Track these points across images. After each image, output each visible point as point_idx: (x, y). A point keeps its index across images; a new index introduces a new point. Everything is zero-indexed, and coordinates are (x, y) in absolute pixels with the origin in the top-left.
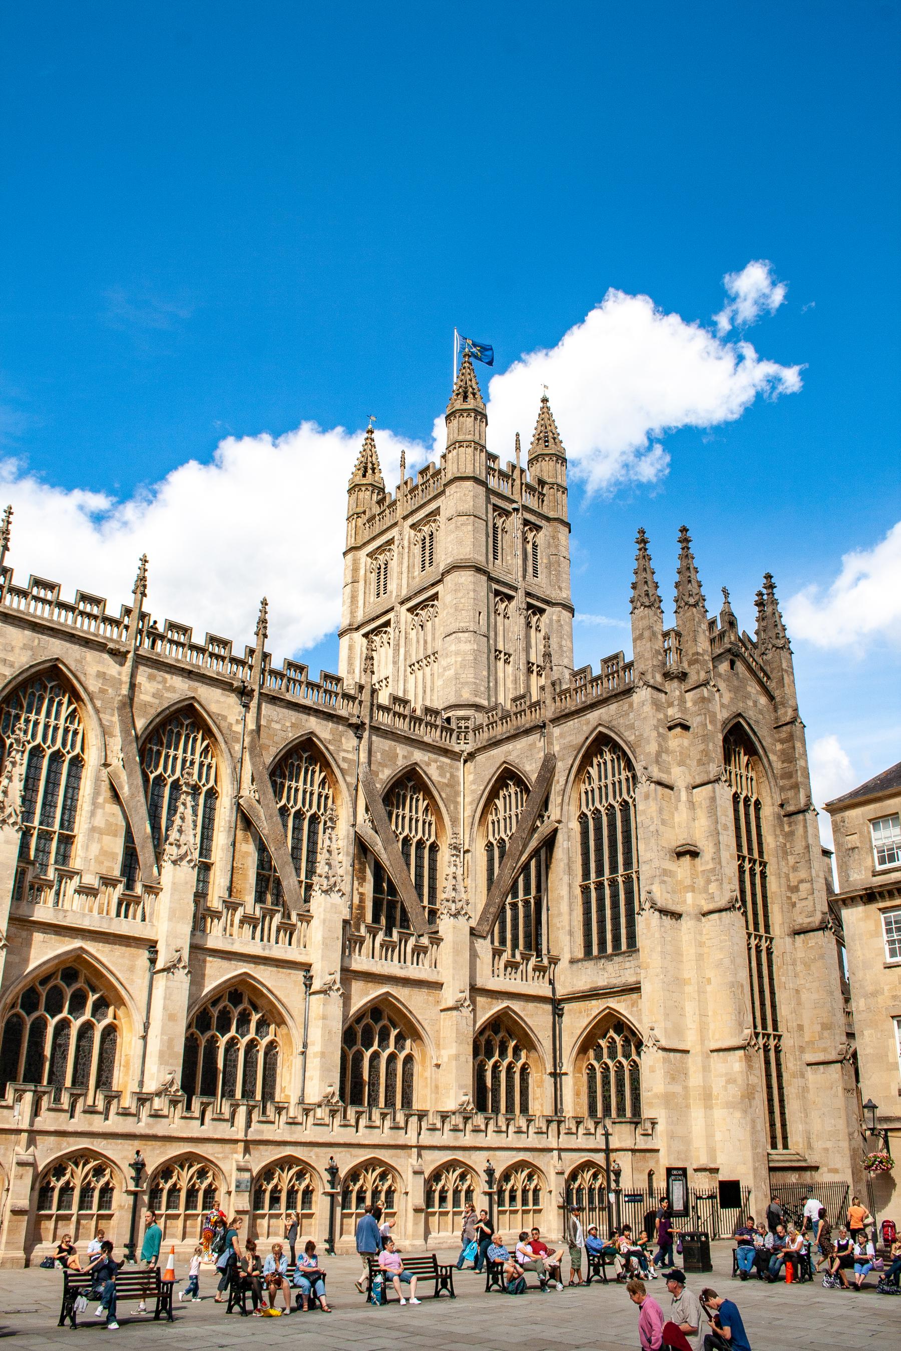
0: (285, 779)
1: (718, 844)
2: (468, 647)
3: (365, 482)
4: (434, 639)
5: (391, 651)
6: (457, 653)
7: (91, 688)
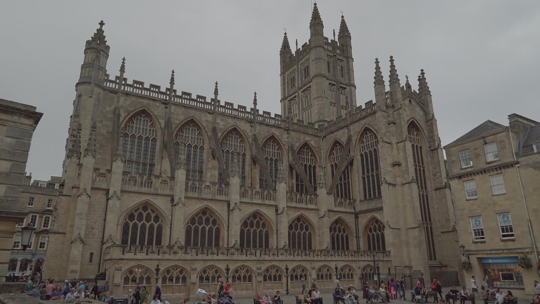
1: (407, 161)
2: (321, 102)
4: (310, 100)
5: (297, 106)
6: (318, 105)
7: (204, 125)
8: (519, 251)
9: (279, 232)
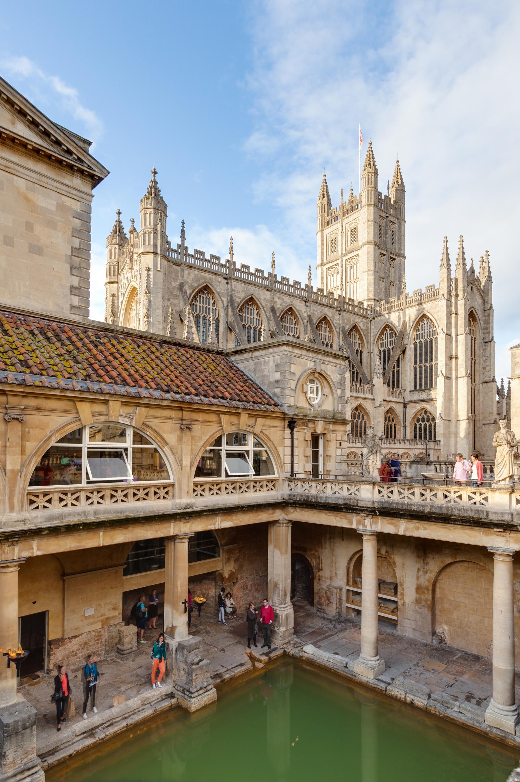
7: (263, 304)
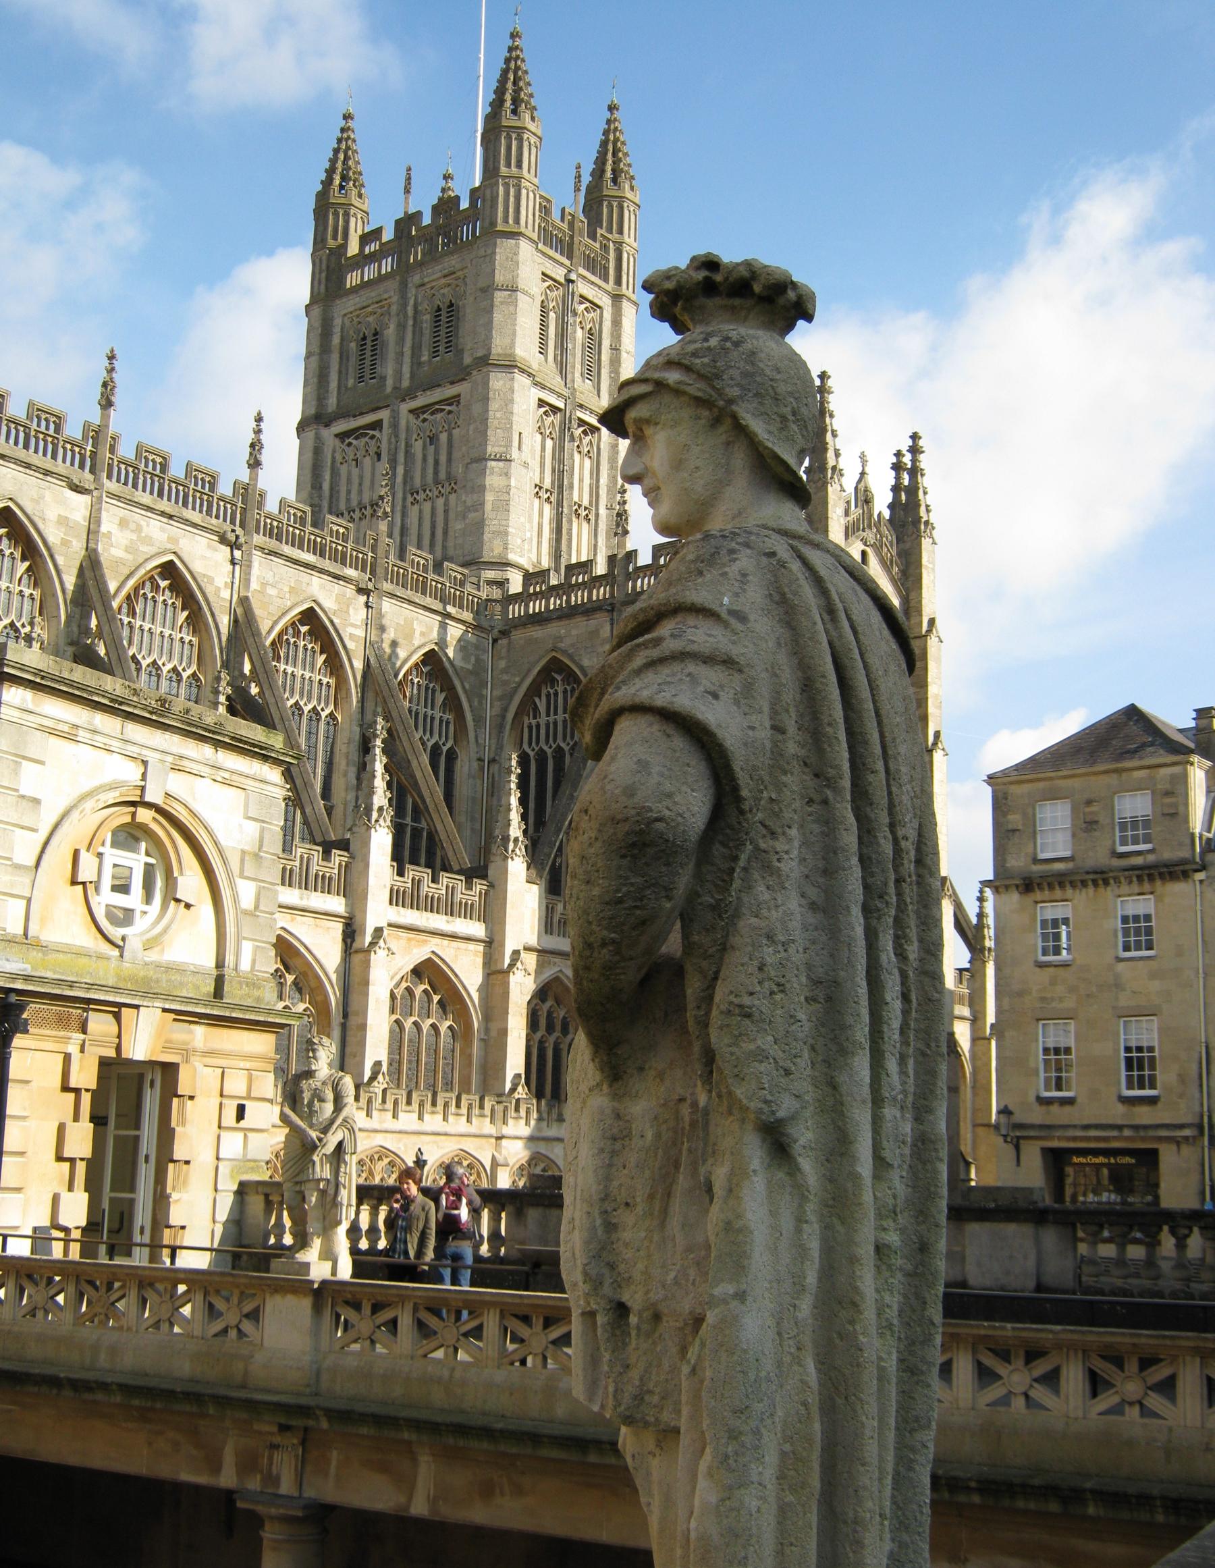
0: (279, 660)
3: (342, 201)
8: (1164, 1133)
9: (353, 1021)
